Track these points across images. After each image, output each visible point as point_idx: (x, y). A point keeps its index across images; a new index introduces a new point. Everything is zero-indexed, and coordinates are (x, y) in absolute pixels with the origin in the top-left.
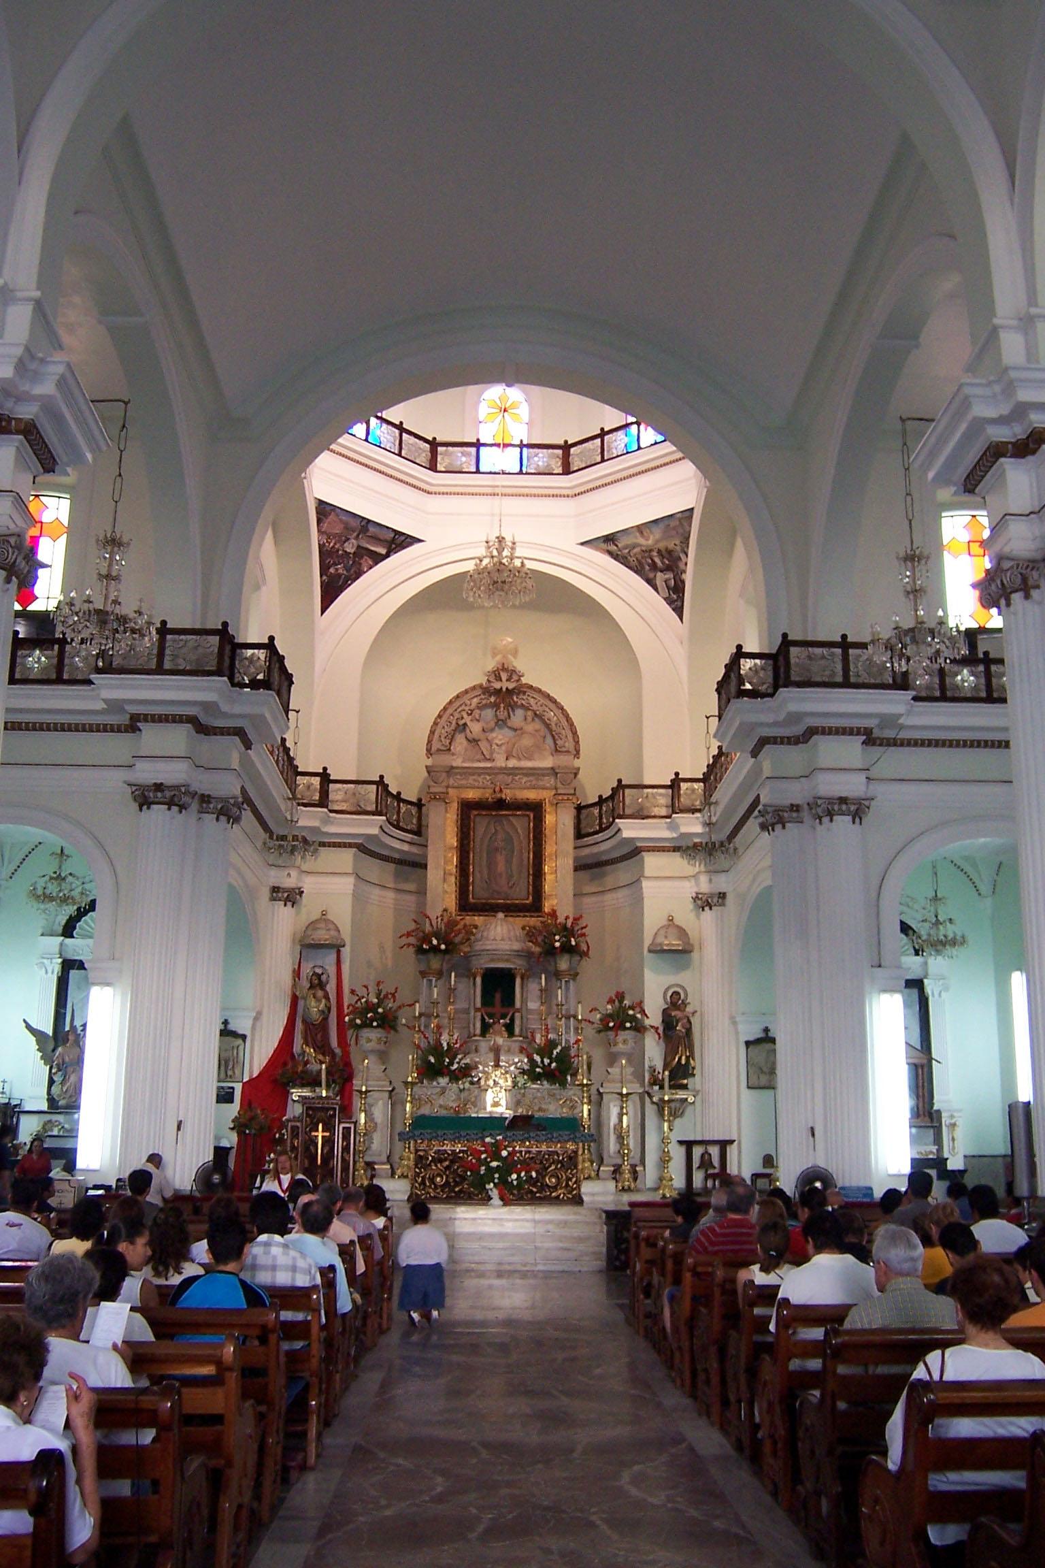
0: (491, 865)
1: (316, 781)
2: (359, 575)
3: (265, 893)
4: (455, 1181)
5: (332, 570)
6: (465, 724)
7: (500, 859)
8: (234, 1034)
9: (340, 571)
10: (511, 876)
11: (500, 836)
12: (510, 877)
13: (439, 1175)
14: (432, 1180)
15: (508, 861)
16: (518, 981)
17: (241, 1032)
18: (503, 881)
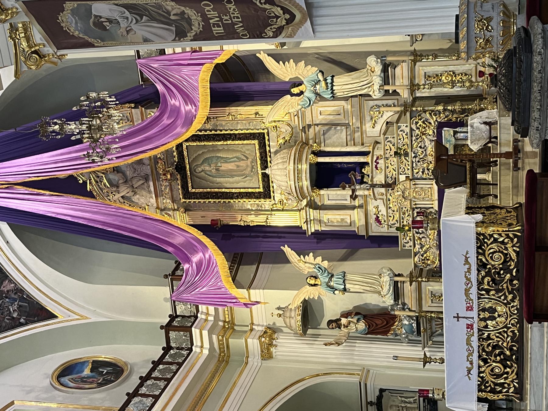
0: (230, 174)
1: (172, 334)
2: (19, 290)
3: (269, 363)
4: (499, 355)
5: (15, 315)
6: (122, 197)
7: (225, 167)
8: (380, 398)
9: (15, 307)
10: (237, 158)
11: (207, 168)
12: (240, 159)
13: (492, 370)
14: (498, 376)
15: (226, 160)
16: (321, 160)
17: (377, 393)
18: (242, 164)
